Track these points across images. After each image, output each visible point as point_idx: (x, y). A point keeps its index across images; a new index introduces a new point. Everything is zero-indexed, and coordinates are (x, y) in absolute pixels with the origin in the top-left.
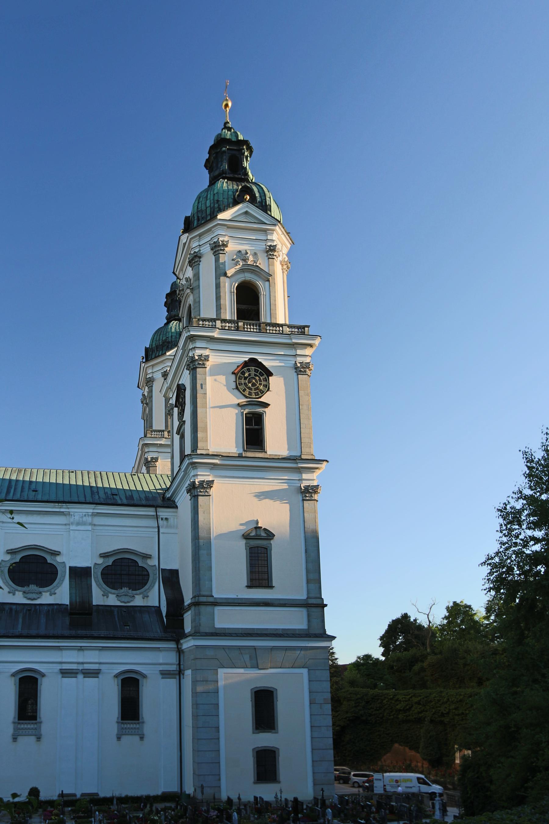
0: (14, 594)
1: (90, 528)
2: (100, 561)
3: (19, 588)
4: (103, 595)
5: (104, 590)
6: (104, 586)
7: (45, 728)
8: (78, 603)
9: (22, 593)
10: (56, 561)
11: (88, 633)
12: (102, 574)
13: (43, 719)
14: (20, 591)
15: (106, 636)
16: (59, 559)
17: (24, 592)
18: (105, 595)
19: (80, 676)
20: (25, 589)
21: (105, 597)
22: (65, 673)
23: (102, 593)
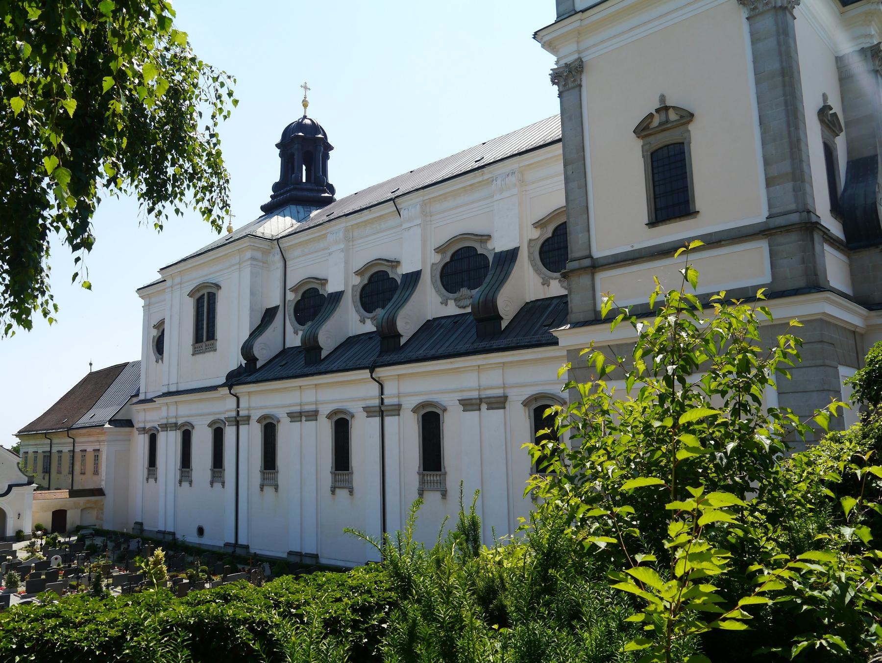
0: (446, 305)
1: (515, 191)
2: (535, 234)
3: (451, 295)
4: (543, 284)
5: (544, 276)
6: (544, 270)
7: (451, 482)
8: (480, 304)
9: (453, 301)
10: (486, 249)
11: (495, 344)
12: (541, 253)
13: (447, 469)
14: (452, 299)
15: (507, 346)
16: (490, 245)
17: (455, 300)
18: (546, 283)
19: (484, 407)
20: (455, 295)
21: (546, 286)
22: (469, 405)
23: (542, 281)
